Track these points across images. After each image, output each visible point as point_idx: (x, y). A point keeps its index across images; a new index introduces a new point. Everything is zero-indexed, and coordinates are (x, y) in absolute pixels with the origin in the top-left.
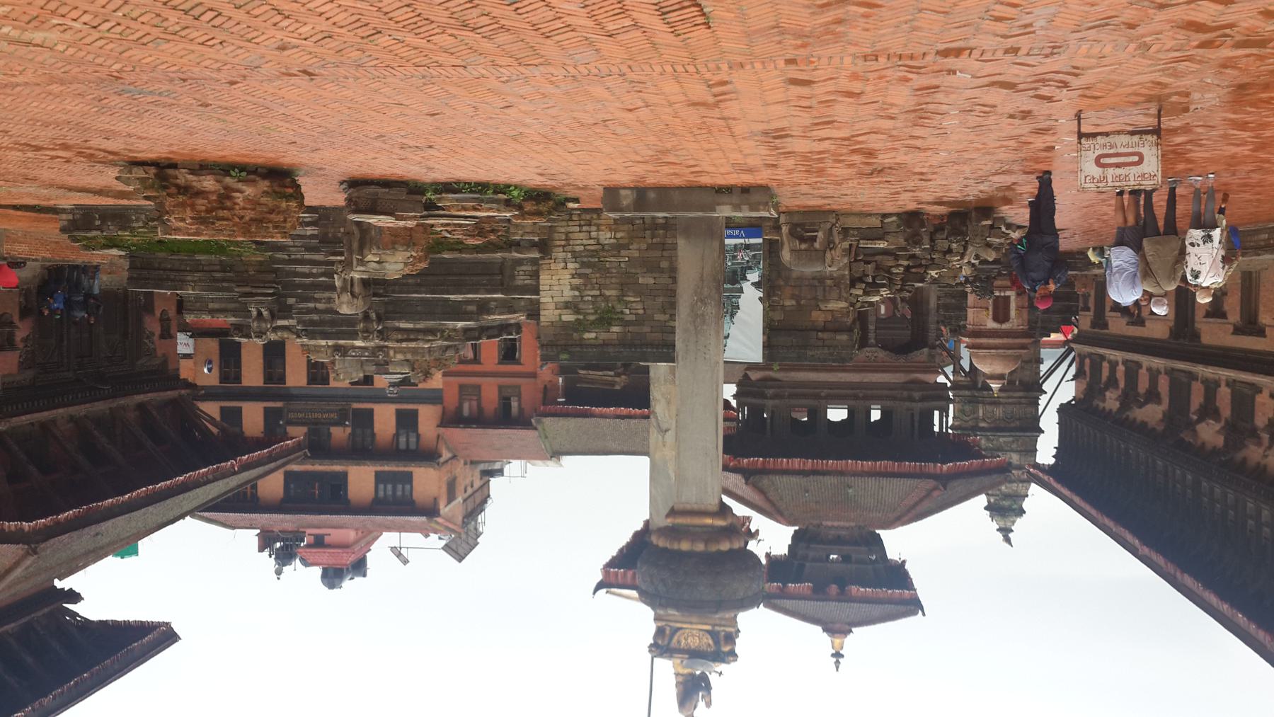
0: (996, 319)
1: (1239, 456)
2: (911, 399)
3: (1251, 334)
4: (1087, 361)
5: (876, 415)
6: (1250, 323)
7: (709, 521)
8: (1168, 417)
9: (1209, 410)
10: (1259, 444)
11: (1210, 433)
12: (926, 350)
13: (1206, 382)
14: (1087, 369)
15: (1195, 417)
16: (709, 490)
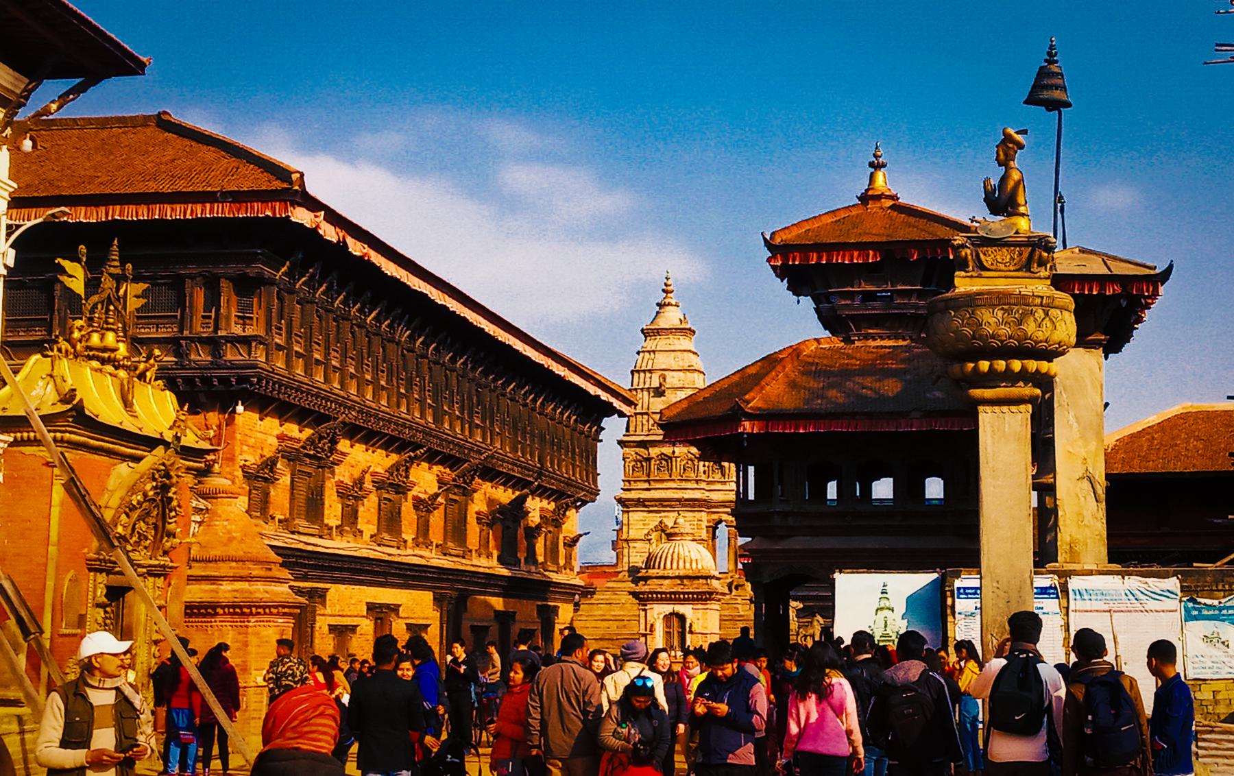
0: (682, 618)
1: (394, 458)
2: (785, 515)
3: (381, 606)
4: (562, 562)
5: (832, 490)
6: (381, 619)
7: (988, 393)
8: (468, 493)
9: (424, 506)
10: (374, 474)
11: (425, 479)
12: (766, 580)
13: (428, 545)
14: (562, 551)
15: (440, 499)
16: (989, 429)
